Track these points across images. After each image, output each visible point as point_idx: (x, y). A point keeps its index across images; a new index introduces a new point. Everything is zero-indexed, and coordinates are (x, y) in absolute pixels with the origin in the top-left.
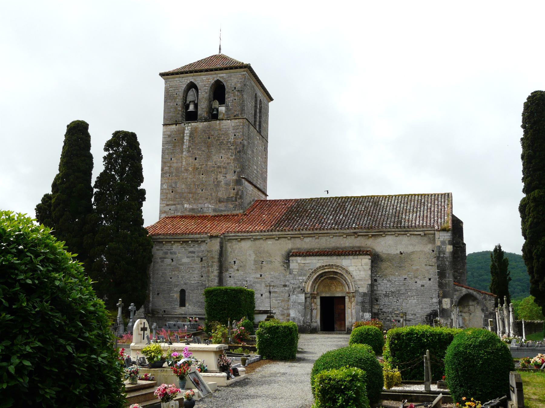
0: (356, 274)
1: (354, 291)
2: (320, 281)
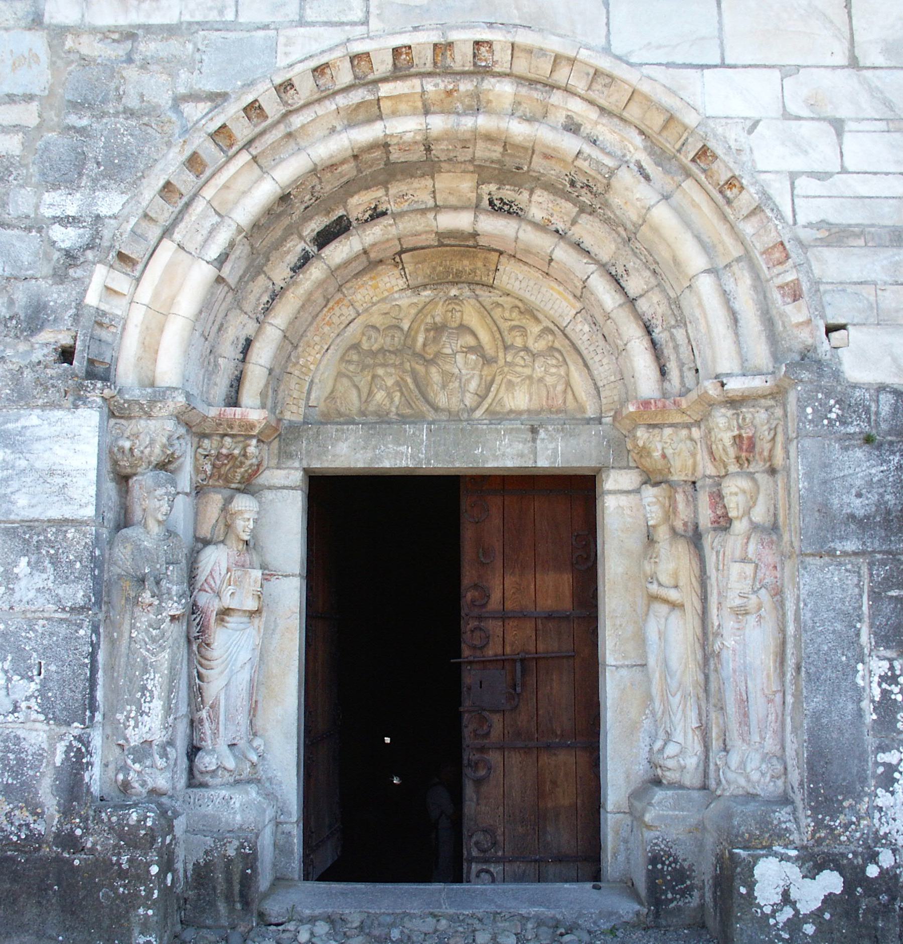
0: (798, 164)
1: (757, 383)
2: (315, 272)
